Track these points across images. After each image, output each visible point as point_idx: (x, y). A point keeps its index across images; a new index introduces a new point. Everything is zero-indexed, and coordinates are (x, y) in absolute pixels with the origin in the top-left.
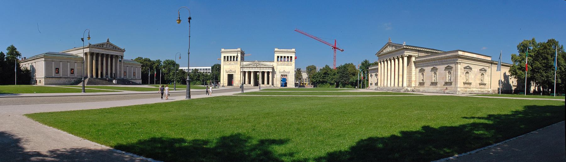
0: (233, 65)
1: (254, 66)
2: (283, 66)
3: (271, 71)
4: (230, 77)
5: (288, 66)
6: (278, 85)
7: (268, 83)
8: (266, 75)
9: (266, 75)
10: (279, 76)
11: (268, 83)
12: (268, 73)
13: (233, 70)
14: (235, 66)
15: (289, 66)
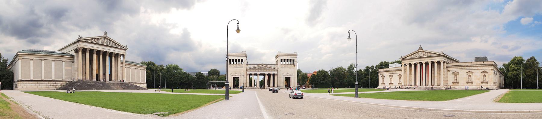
0: (239, 68)
1: (260, 68)
2: (286, 69)
3: (277, 73)
4: (288, 79)
5: (291, 69)
6: (282, 87)
7: (274, 86)
8: (272, 77)
9: (272, 77)
10: (283, 78)
11: (274, 86)
12: (274, 75)
13: (239, 73)
14: (240, 68)
15: (292, 69)
